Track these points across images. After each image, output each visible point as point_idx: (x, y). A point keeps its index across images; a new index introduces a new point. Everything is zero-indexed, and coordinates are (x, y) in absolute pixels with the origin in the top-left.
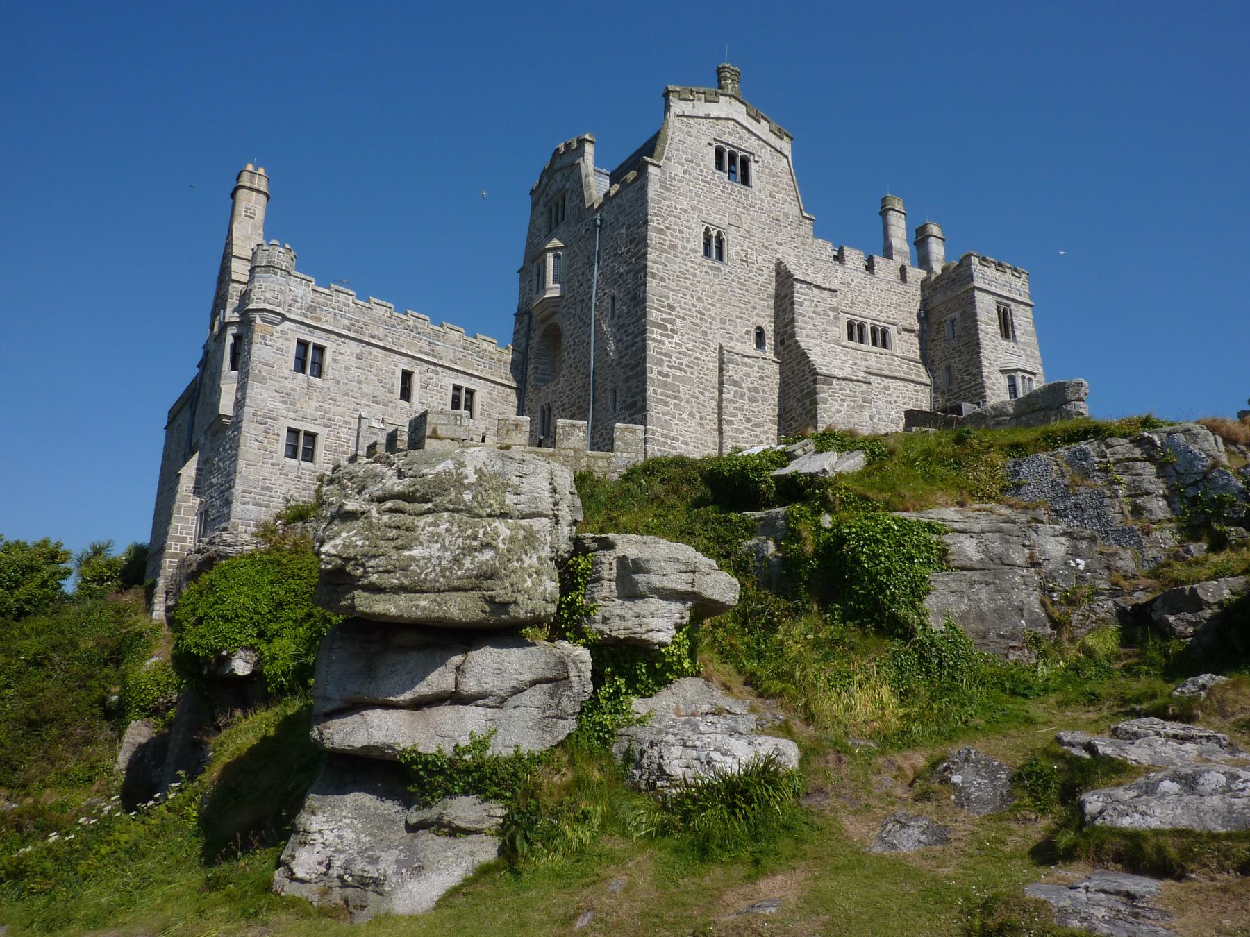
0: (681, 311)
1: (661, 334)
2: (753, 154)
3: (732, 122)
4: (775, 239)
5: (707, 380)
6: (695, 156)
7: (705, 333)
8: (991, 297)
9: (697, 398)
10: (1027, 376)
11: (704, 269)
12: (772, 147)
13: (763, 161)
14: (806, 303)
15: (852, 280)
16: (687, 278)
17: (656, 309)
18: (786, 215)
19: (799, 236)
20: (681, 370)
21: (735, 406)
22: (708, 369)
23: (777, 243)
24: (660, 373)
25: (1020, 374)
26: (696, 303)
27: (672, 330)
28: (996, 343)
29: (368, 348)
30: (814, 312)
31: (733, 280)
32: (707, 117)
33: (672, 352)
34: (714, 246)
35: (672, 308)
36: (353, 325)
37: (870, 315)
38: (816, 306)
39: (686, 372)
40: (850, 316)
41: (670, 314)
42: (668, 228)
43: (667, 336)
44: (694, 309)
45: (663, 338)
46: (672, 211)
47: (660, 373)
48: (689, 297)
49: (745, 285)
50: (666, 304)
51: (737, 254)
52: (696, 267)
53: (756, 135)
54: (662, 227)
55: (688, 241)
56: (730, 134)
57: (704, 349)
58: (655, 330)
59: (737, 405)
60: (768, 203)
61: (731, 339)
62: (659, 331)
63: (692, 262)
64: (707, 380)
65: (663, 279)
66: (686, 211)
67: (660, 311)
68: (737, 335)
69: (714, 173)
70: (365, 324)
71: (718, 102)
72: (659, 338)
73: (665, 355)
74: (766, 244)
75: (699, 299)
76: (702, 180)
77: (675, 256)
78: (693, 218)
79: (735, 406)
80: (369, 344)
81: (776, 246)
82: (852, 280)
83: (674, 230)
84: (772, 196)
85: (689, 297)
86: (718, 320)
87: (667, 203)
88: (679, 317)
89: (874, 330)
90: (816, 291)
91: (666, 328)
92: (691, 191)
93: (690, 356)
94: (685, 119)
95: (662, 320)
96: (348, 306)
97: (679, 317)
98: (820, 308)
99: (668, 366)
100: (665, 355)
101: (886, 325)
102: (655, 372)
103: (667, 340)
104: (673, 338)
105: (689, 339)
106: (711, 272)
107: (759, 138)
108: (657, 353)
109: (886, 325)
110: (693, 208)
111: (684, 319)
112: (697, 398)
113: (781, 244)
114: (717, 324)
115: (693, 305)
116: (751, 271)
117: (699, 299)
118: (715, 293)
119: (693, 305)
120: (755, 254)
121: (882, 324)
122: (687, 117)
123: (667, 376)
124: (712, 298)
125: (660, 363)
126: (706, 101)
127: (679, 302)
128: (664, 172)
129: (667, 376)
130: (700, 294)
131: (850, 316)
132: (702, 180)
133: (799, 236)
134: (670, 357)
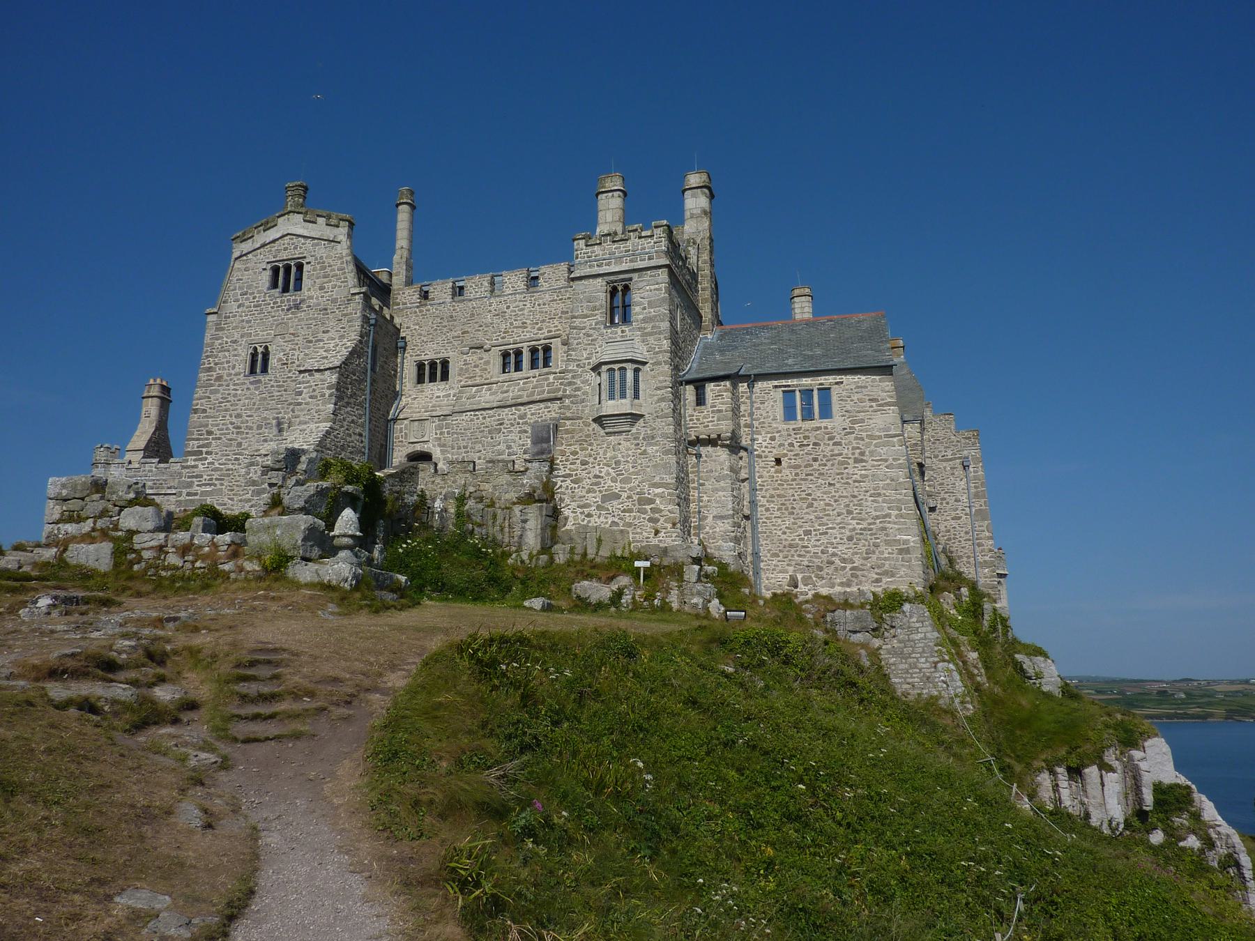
0: (218, 432)
1: (195, 460)
2: (305, 257)
3: (289, 237)
4: (322, 329)
5: (237, 486)
6: (249, 287)
7: (240, 445)
8: (600, 280)
9: (225, 504)
10: (616, 366)
11: (245, 386)
12: (326, 240)
13: (316, 259)
14: (305, 390)
15: (508, 307)
16: (228, 402)
17: (194, 439)
18: (334, 301)
19: (345, 315)
20: (210, 485)
21: (250, 504)
22: (239, 476)
23: (324, 332)
24: (188, 494)
25: (604, 368)
26: (234, 420)
27: (207, 453)
28: (595, 337)
29: (166, 497)
30: (311, 397)
31: (272, 386)
32: (263, 246)
33: (204, 471)
34: (259, 362)
35: (209, 433)
36: (155, 484)
37: (524, 338)
38: (314, 390)
39: (215, 485)
40: (502, 348)
41: (207, 439)
42: (216, 364)
43: (201, 460)
44: (230, 426)
45: (197, 463)
46: (223, 347)
47: (188, 494)
48: (228, 417)
49: (283, 386)
50: (204, 432)
51: (280, 360)
52: (237, 387)
53: (310, 238)
54: (212, 365)
55: (234, 367)
56: (285, 249)
57: (237, 459)
58: (190, 458)
59: (253, 502)
60: (317, 298)
61: (265, 441)
62: (194, 457)
63: (234, 385)
64: (237, 486)
65: (204, 411)
66: (235, 342)
67: (198, 439)
68: (271, 435)
69: (266, 294)
70: (165, 480)
71: (276, 225)
72: (193, 463)
73: (196, 477)
74: (311, 338)
75: (238, 416)
76: (255, 306)
77: (219, 386)
78: (241, 345)
79: (250, 504)
80: (165, 494)
81: (320, 335)
82: (508, 307)
83: (221, 364)
84: (321, 288)
85: (228, 417)
86: (255, 428)
87: (220, 341)
88: (216, 439)
89: (534, 351)
90: (317, 375)
91: (201, 453)
92: (243, 321)
93: (222, 469)
94: (245, 258)
95: (198, 447)
96: (151, 471)
97: (216, 439)
98: (317, 391)
99: (198, 485)
100: (196, 477)
101: (547, 341)
102: (184, 495)
103: (199, 463)
104: (206, 459)
105: (223, 455)
106: (252, 387)
107: (314, 238)
108: (189, 477)
109: (547, 341)
110: (242, 336)
111: (219, 439)
112: (225, 504)
113: (328, 331)
114: (255, 431)
115: (232, 423)
116: (290, 371)
117: (238, 416)
118: (254, 404)
119: (232, 423)
120: (296, 354)
121: (542, 342)
122: (245, 255)
123: (196, 494)
124: (251, 409)
125: (190, 485)
126: (264, 231)
127: (217, 425)
128: (220, 316)
129: (196, 494)
130: (239, 411)
131: (502, 348)
132: (255, 306)
133: (345, 315)
134: (202, 476)
